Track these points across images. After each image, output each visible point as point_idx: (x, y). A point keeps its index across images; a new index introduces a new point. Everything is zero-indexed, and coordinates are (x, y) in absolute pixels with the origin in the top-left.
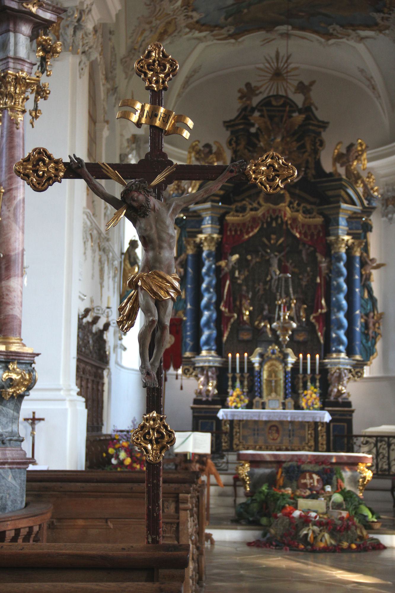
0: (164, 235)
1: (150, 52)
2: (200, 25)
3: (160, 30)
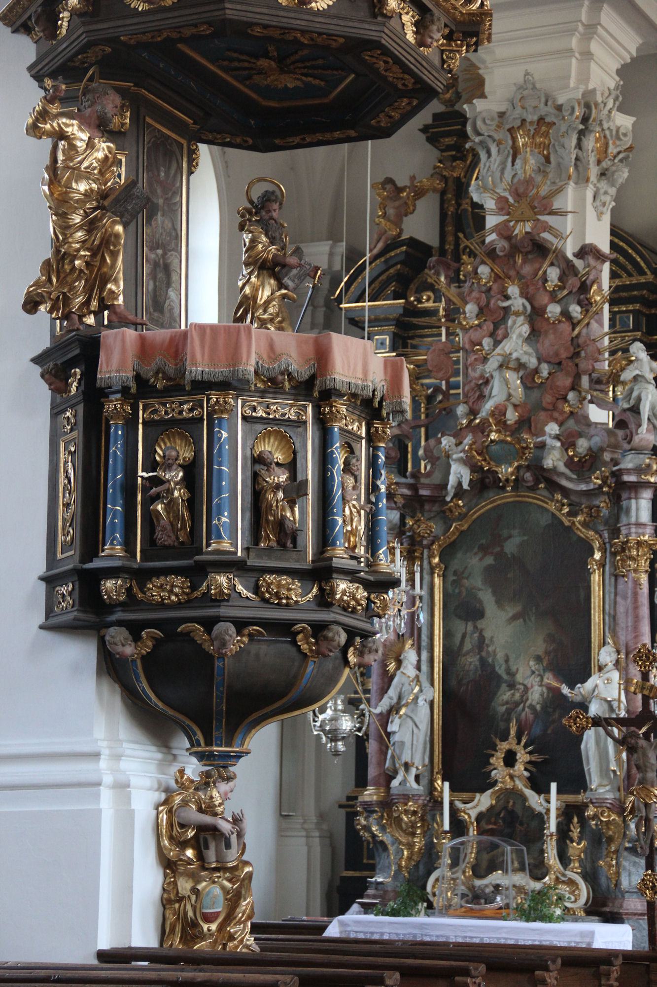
0: (648, 765)
1: (640, 649)
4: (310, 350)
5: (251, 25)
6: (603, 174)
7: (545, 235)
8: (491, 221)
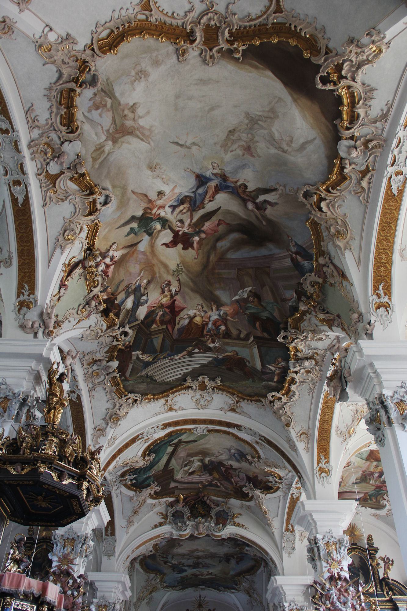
2: (167, 587)
3: (150, 590)
4: (41, 586)
5: (45, 484)
6: (86, 556)
7: (70, 570)
8: (54, 564)
